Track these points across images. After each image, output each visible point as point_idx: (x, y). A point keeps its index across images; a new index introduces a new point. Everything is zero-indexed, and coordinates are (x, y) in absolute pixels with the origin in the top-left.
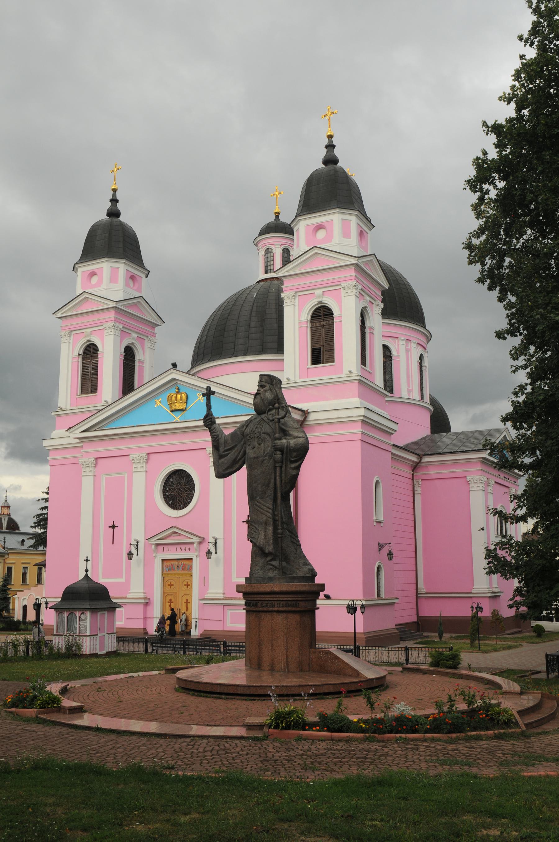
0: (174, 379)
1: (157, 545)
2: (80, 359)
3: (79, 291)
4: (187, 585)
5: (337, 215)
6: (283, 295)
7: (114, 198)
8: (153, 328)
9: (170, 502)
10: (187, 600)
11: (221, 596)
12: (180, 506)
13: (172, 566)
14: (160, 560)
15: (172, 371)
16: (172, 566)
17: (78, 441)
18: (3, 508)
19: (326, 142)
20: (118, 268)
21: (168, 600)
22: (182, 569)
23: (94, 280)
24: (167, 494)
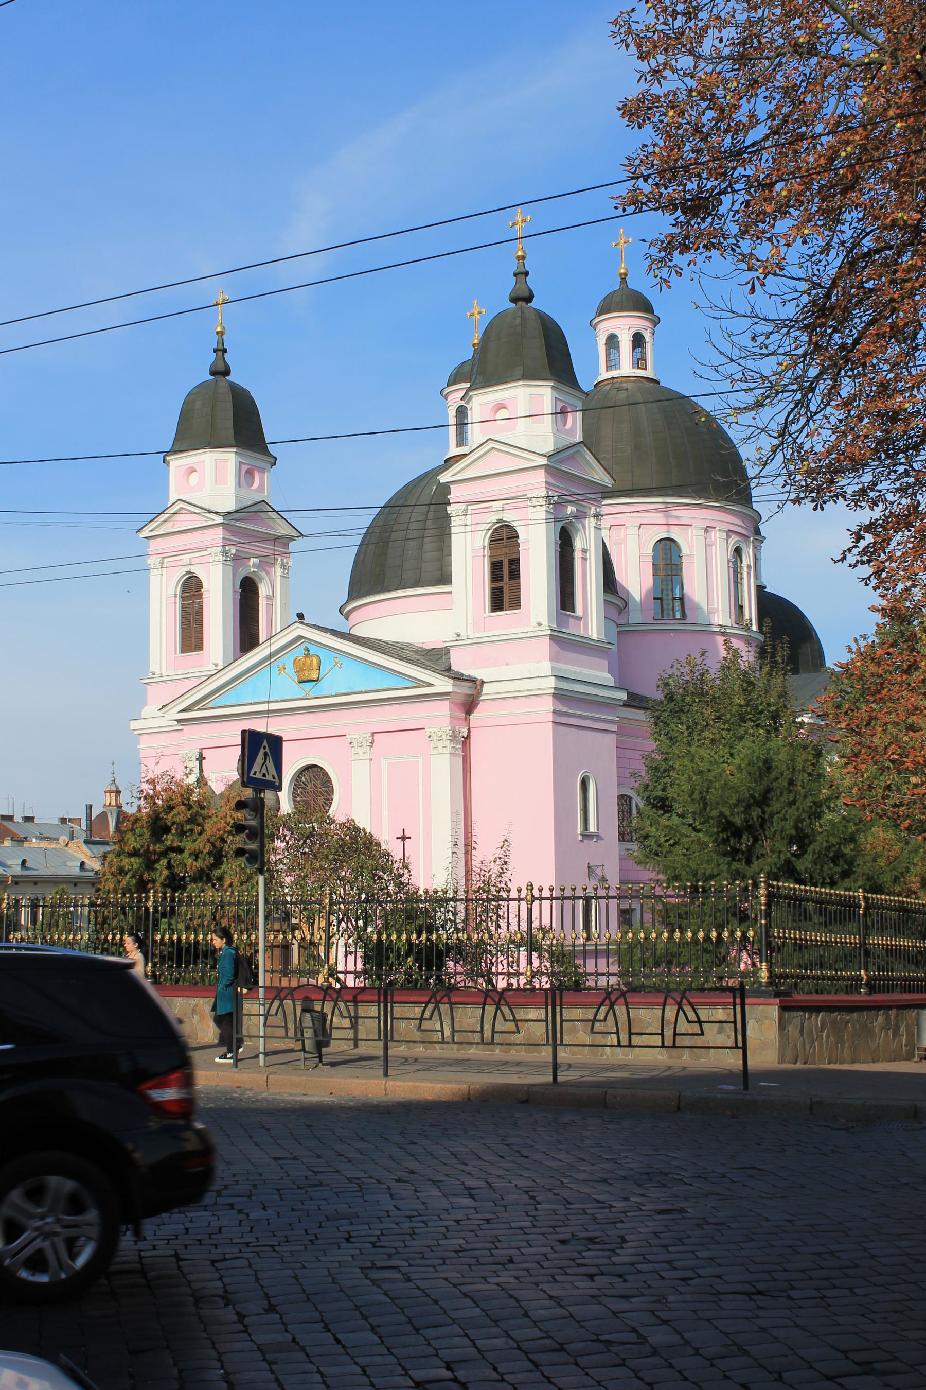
0: (300, 637)
3: (172, 499)
5: (523, 388)
6: (450, 509)
7: (220, 347)
8: (286, 545)
15: (297, 625)
17: (176, 723)
18: (108, 794)
19: (514, 267)
23: (194, 478)
24: (299, 799)
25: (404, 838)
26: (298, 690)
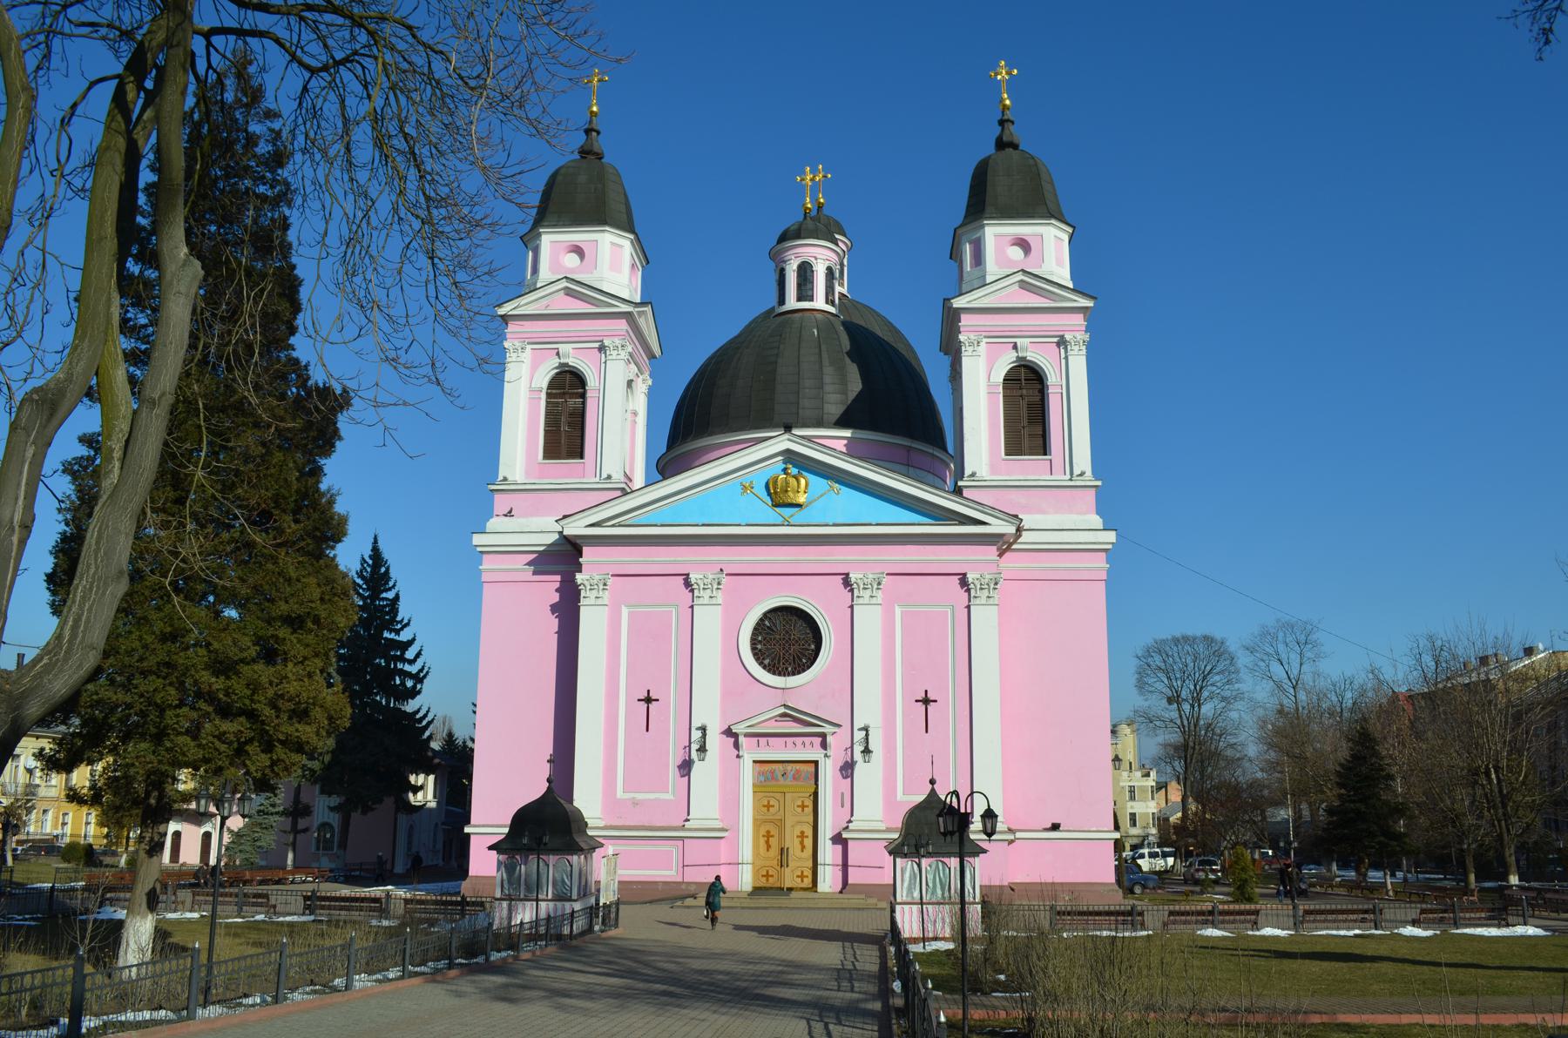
1: (747, 735)
2: (543, 396)
4: (803, 807)
9: (766, 662)
10: (802, 833)
11: (882, 826)
12: (787, 669)
13: (772, 772)
14: (751, 763)
16: (772, 772)
20: (621, 246)
21: (763, 832)
22: (794, 778)
24: (759, 647)
25: (926, 701)
26: (773, 515)
